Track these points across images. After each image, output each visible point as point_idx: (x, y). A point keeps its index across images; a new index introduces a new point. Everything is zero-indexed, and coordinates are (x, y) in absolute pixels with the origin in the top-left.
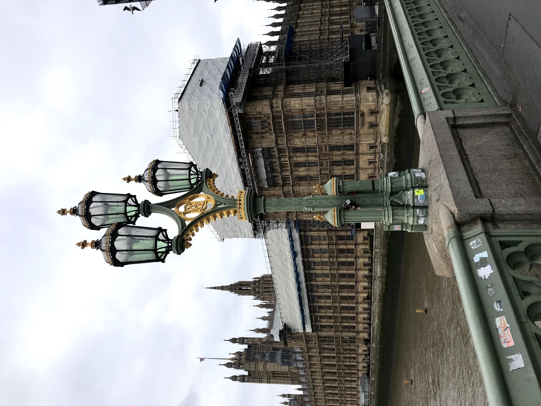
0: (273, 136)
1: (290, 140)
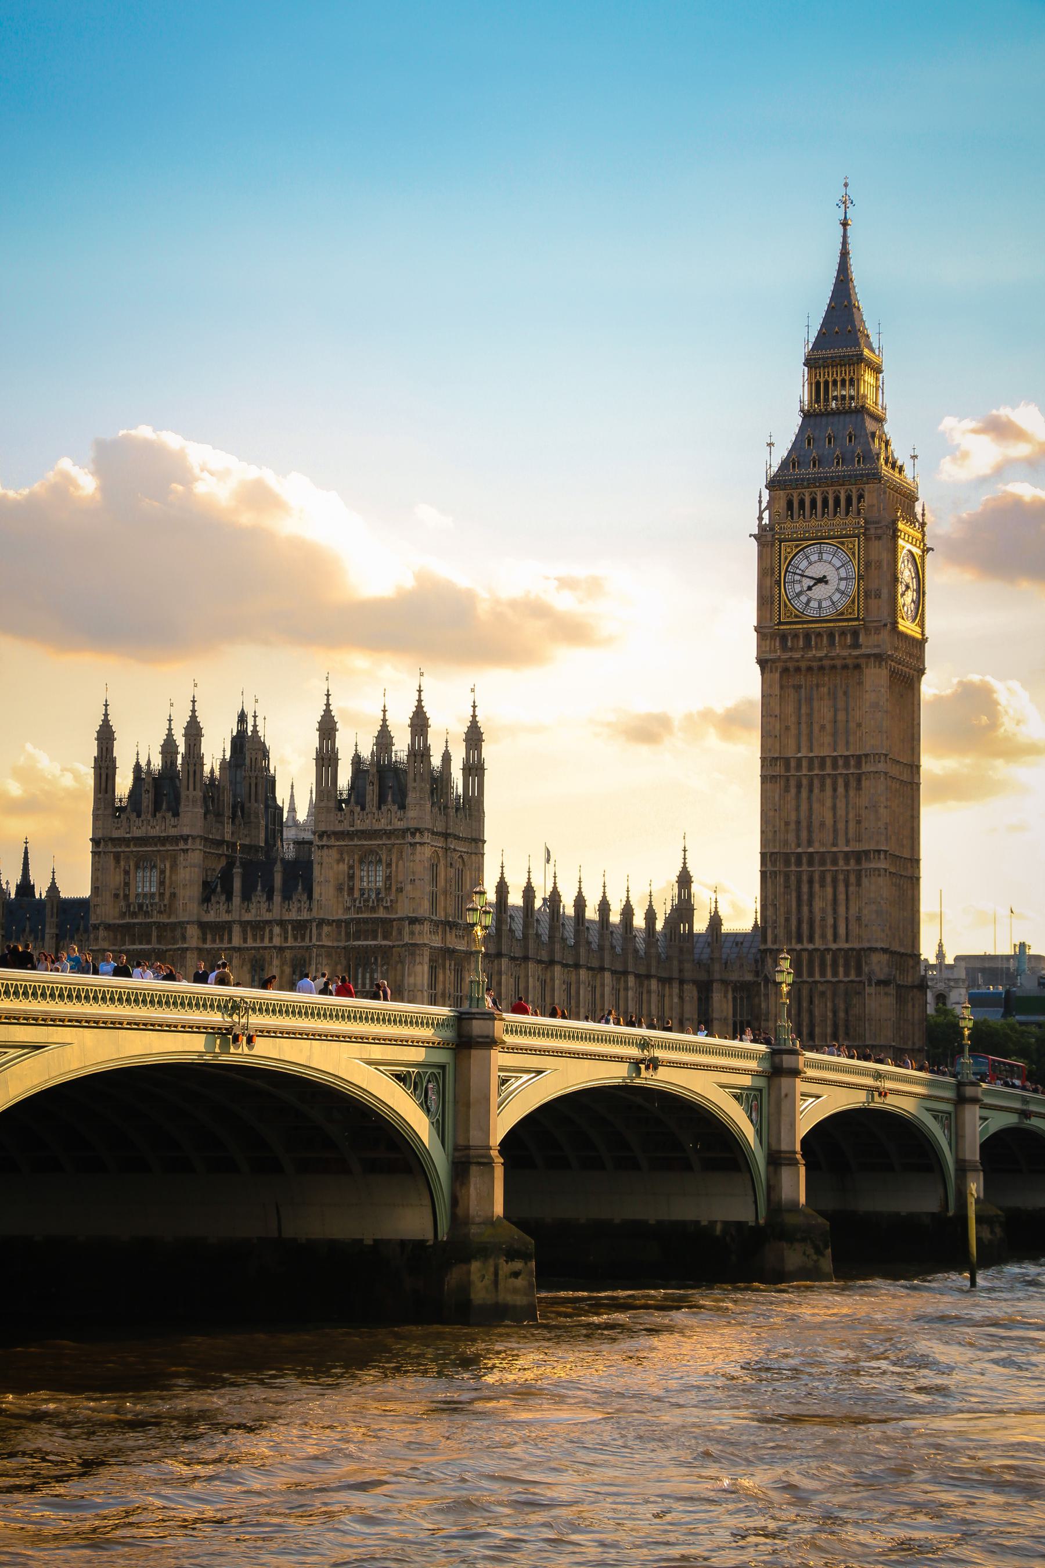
0: (340, 915)
1: (329, 956)
